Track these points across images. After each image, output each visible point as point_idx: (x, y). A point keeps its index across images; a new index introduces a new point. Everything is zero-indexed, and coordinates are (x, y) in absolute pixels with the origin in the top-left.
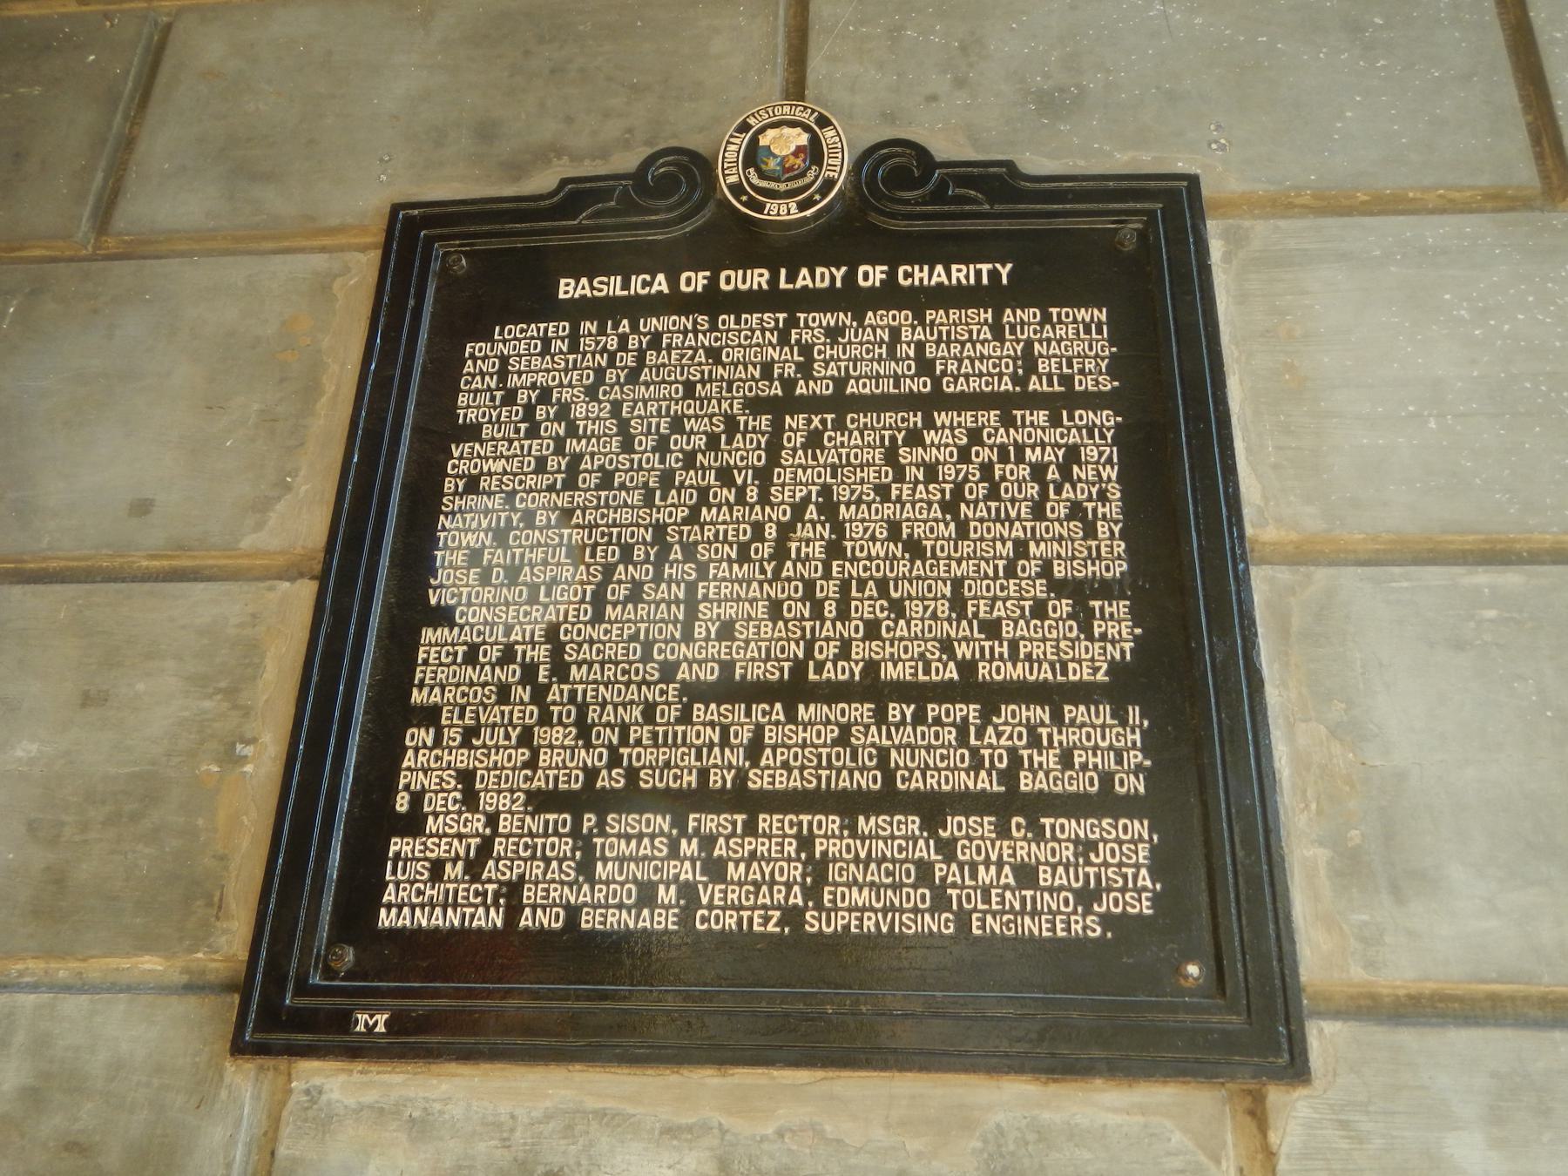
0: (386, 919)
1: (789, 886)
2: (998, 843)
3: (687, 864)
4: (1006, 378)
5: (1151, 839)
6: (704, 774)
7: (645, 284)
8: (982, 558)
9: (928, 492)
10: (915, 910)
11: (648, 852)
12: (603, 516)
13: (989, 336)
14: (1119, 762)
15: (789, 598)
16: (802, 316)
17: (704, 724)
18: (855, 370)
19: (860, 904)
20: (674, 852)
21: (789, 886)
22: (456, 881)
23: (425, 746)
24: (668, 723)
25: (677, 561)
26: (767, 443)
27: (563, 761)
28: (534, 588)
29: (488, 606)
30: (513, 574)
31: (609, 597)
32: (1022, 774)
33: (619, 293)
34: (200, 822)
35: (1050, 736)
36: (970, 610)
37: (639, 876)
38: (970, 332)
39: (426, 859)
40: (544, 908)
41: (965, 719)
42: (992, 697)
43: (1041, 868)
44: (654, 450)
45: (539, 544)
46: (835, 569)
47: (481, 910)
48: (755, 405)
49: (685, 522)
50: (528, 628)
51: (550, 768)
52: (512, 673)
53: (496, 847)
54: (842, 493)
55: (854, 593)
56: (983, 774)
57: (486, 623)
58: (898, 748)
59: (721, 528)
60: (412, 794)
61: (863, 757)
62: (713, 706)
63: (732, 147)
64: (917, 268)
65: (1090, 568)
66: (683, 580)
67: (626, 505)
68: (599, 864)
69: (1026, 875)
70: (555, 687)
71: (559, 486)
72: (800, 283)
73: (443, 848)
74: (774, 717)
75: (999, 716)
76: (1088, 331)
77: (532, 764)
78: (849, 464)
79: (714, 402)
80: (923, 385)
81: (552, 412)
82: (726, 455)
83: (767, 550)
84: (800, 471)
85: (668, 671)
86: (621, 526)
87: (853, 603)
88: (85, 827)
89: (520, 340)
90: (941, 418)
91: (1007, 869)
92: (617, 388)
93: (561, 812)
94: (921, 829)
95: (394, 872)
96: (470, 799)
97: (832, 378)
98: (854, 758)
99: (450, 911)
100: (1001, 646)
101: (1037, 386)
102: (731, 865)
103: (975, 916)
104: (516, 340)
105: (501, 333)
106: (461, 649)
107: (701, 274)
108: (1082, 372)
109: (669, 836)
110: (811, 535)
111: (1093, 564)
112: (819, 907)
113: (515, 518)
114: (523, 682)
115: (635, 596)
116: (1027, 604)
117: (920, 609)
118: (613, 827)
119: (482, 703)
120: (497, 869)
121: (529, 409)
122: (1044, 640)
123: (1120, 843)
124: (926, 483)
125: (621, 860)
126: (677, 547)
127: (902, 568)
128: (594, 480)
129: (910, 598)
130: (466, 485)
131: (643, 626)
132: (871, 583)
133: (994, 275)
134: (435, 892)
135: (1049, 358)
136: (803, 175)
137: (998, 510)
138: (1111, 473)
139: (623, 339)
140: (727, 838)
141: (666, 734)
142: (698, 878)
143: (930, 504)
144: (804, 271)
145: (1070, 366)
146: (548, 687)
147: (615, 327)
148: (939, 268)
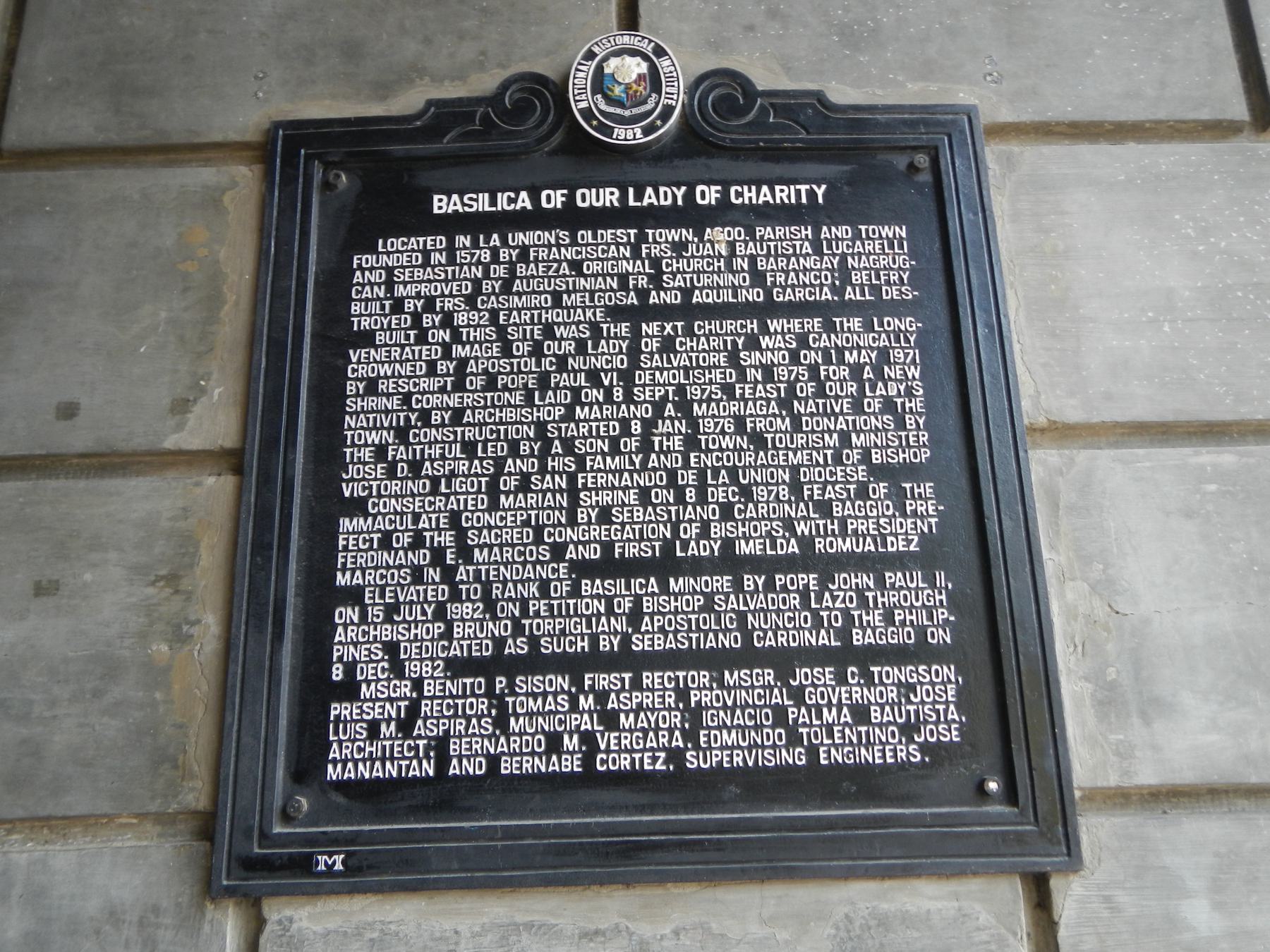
0: (332, 773)
1: (671, 731)
2: (837, 689)
3: (586, 717)
4: (825, 289)
5: (957, 680)
6: (594, 639)
7: (510, 201)
8: (814, 448)
9: (766, 391)
10: (774, 746)
11: (553, 707)
12: (491, 415)
13: (810, 251)
14: (930, 618)
15: (656, 486)
16: (650, 232)
17: (592, 597)
18: (699, 281)
19: (730, 744)
20: (574, 707)
21: (671, 731)
22: (391, 738)
23: (352, 623)
24: (561, 597)
25: (557, 454)
26: (628, 348)
27: (474, 632)
28: (435, 481)
29: (396, 496)
30: (416, 467)
31: (502, 488)
32: (854, 631)
33: (487, 208)
34: (158, 695)
35: (875, 598)
36: (806, 493)
37: (546, 728)
38: (794, 247)
39: (362, 720)
40: (468, 757)
41: (807, 586)
42: (828, 566)
43: (872, 708)
44: (530, 355)
45: (437, 441)
46: (693, 460)
47: (415, 762)
48: (616, 313)
49: (563, 419)
50: (434, 516)
51: (463, 638)
52: (422, 557)
53: (423, 708)
54: (694, 392)
55: (710, 482)
56: (823, 632)
57: (396, 513)
58: (753, 612)
59: (594, 424)
60: (346, 665)
61: (726, 620)
62: (598, 582)
64: (746, 188)
65: (901, 456)
66: (565, 472)
67: (510, 405)
68: (512, 720)
69: (861, 714)
70: (462, 568)
71: (449, 388)
72: (646, 202)
73: (377, 710)
74: (650, 590)
75: (834, 583)
76: (891, 246)
77: (448, 635)
78: (699, 366)
79: (579, 311)
80: (754, 295)
81: (437, 320)
82: (593, 359)
83: (634, 444)
84: (657, 374)
85: (558, 551)
86: (507, 423)
87: (710, 490)
88: (53, 703)
89: (402, 252)
90: (774, 325)
91: (845, 710)
92: (493, 298)
93: (476, 676)
94: (775, 679)
95: (336, 733)
96: (397, 669)
97: (680, 288)
98: (718, 622)
99: (388, 765)
100: (833, 524)
101: (852, 296)
102: (622, 716)
103: (822, 749)
104: (398, 251)
105: (385, 246)
106: (376, 536)
107: (559, 192)
108: (888, 283)
109: (569, 693)
110: (671, 430)
111: (904, 452)
112: (697, 747)
113: (413, 417)
114: (433, 564)
115: (525, 485)
116: (852, 487)
117: (765, 493)
118: (521, 688)
119: (399, 584)
120: (426, 727)
121: (417, 317)
122: (867, 517)
123: (933, 684)
124: (764, 383)
125: (530, 714)
126: (557, 442)
127: (748, 459)
128: (480, 382)
129: (757, 484)
130: (365, 388)
131: (533, 513)
132: (723, 472)
133: (812, 195)
134: (374, 749)
135: (859, 269)
136: (645, 102)
137: (825, 405)
138: (914, 372)
139: (495, 252)
140: (618, 693)
141: (560, 605)
142: (596, 728)
143: (768, 400)
144: (649, 190)
145: (878, 278)
146: (454, 569)
147: (487, 241)
148: (765, 189)
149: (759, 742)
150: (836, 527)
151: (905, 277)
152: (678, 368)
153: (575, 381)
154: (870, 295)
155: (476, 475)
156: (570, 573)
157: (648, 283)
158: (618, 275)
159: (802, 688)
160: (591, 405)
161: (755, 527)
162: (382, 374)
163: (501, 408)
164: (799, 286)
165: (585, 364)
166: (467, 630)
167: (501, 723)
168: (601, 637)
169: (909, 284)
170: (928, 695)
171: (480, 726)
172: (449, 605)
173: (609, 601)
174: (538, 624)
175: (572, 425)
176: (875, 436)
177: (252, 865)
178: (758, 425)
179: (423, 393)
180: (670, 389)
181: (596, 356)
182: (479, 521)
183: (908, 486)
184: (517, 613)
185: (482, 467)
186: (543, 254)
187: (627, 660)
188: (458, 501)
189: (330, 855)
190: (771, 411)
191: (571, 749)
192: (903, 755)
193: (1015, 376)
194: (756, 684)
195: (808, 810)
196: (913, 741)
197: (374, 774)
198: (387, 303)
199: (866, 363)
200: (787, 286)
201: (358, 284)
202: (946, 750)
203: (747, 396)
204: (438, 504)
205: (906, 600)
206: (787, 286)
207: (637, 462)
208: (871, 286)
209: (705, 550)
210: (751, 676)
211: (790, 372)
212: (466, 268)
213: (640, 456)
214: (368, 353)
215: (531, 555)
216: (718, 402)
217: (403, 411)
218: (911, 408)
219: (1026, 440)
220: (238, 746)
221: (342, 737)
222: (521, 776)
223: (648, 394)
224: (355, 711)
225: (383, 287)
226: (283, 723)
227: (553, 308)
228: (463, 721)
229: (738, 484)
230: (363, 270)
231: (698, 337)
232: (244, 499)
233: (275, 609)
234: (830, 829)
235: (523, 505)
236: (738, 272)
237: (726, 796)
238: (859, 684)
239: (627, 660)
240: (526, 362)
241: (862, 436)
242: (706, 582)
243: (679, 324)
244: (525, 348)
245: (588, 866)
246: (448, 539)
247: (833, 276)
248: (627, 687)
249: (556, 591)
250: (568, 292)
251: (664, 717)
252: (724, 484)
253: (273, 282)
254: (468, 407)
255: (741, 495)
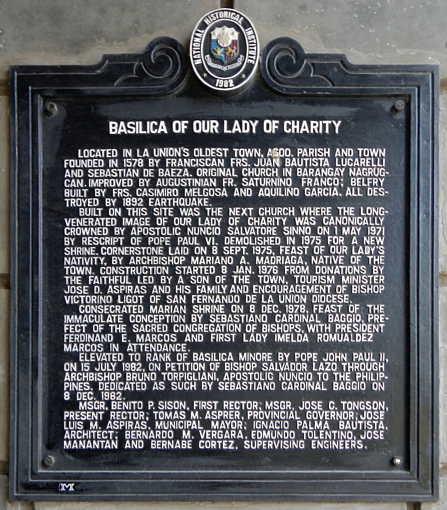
0: (66, 445)
1: (237, 430)
2: (323, 412)
3: (194, 422)
4: (335, 189)
5: (385, 409)
6: (199, 384)
7: (155, 127)
8: (321, 284)
9: (297, 250)
11: (177, 417)
12: (145, 260)
13: (328, 165)
14: (375, 377)
15: (234, 303)
16: (236, 150)
17: (198, 362)
18: (263, 183)
19: (266, 437)
20: (188, 417)
21: (237, 430)
22: (95, 429)
23: (73, 371)
24: (182, 362)
25: (181, 284)
26: (221, 223)
27: (136, 378)
28: (115, 297)
29: (94, 304)
30: (104, 288)
31: (151, 302)
32: (334, 383)
33: (141, 132)
35: (347, 366)
36: (315, 309)
37: (174, 427)
38: (319, 161)
39: (81, 420)
42: (324, 349)
43: (340, 422)
44: (166, 225)
45: (115, 274)
46: (254, 289)
47: (108, 442)
48: (215, 201)
49: (184, 264)
50: (115, 316)
51: (131, 381)
52: (109, 338)
53: (111, 416)
54: (257, 250)
55: (263, 302)
56: (318, 383)
57: (94, 313)
59: (201, 267)
60: (71, 392)
62: (202, 354)
63: (197, 40)
64: (293, 122)
65: (368, 289)
66: (185, 294)
67: (155, 255)
68: (157, 423)
69: (334, 425)
70: (130, 344)
71: (121, 244)
73: (88, 416)
74: (229, 359)
75: (326, 358)
76: (376, 163)
77: (123, 379)
78: (260, 235)
79: (194, 199)
80: (294, 192)
81: (114, 202)
82: (201, 229)
83: (223, 279)
84: (237, 238)
85: (181, 337)
86: (154, 265)
87: (263, 306)
89: (92, 159)
90: (304, 211)
91: (326, 423)
92: (145, 190)
93: (138, 400)
94: (292, 406)
95: (68, 426)
96: (98, 395)
97: (251, 187)
98: (264, 377)
99: (94, 442)
100: (328, 326)
101: (350, 194)
102: (213, 423)
103: (313, 441)
105: (82, 154)
106: (84, 326)
107: (184, 122)
109: (186, 410)
110: (243, 272)
111: (370, 287)
112: (250, 439)
113: (102, 260)
114: (115, 342)
115: (163, 301)
116: (340, 306)
117: (293, 309)
118: (161, 407)
119: (97, 352)
120: (113, 425)
122: (346, 323)
123: (373, 411)
124: (296, 246)
125: (166, 420)
126: (181, 277)
127: (285, 289)
128: (138, 241)
130: (75, 242)
131: (168, 316)
132: (271, 296)
133: (332, 127)
134: (87, 435)
135: (356, 177)
138: (380, 241)
139: (146, 160)
140: (211, 411)
141: (181, 366)
142: (199, 428)
143: (298, 256)
144: (236, 123)
145: (366, 182)
146: (126, 345)
147: (141, 154)
148: (305, 123)
149: (281, 437)
150: (329, 328)
151: (382, 182)
152: (249, 236)
153: (191, 242)
154: (360, 193)
155: (137, 294)
156: (187, 349)
157: (234, 183)
158: (217, 177)
159: (305, 411)
160: (200, 256)
161: (286, 327)
162: (84, 234)
163: (150, 256)
164: (320, 187)
165: (197, 232)
166: (133, 377)
167: (151, 424)
168: (203, 383)
169: (384, 187)
170: (370, 416)
171: (140, 425)
172: (123, 364)
173: (207, 364)
174: (170, 375)
175: (189, 267)
176: (356, 278)
177: (28, 487)
178: (291, 270)
179: (107, 246)
180: (244, 248)
181: (203, 227)
182: (139, 320)
183: (370, 306)
184: (159, 369)
185: (140, 290)
186: (173, 163)
187: (215, 394)
188: (127, 308)
189: (67, 483)
190: (299, 262)
191: (186, 438)
192: (354, 445)
193: (438, 243)
194: (281, 408)
195: (304, 470)
196: (360, 439)
197: (88, 446)
198: (85, 190)
199: (354, 235)
200: (313, 186)
201: (68, 178)
202: (376, 443)
203: (286, 253)
204: (116, 309)
205: (363, 368)
206: (313, 186)
207: (224, 289)
208: (362, 187)
209: (259, 339)
210: (279, 405)
211: (311, 239)
212: (129, 170)
213: (226, 286)
214: (75, 221)
215: (167, 339)
216: (270, 256)
217: (96, 256)
218: (377, 262)
219: (438, 280)
220: (18, 431)
221: (70, 428)
222: (161, 450)
223: (231, 250)
224: (77, 416)
225: (82, 180)
226: (40, 420)
227: (179, 197)
228: (132, 423)
229: (278, 303)
230: (70, 169)
231: (261, 217)
232: (12, 302)
233: (32, 362)
234: (314, 479)
235: (162, 311)
236: (285, 177)
237: (263, 462)
238: (334, 410)
239: (215, 394)
240: (164, 230)
241: (348, 277)
242: (259, 356)
243: (250, 209)
244: (164, 221)
245: (194, 493)
246: (123, 329)
247: (340, 181)
248: (215, 408)
249: (179, 358)
250: (188, 188)
251: (234, 424)
252: (271, 303)
253: (18, 174)
254: (132, 255)
255: (279, 309)
